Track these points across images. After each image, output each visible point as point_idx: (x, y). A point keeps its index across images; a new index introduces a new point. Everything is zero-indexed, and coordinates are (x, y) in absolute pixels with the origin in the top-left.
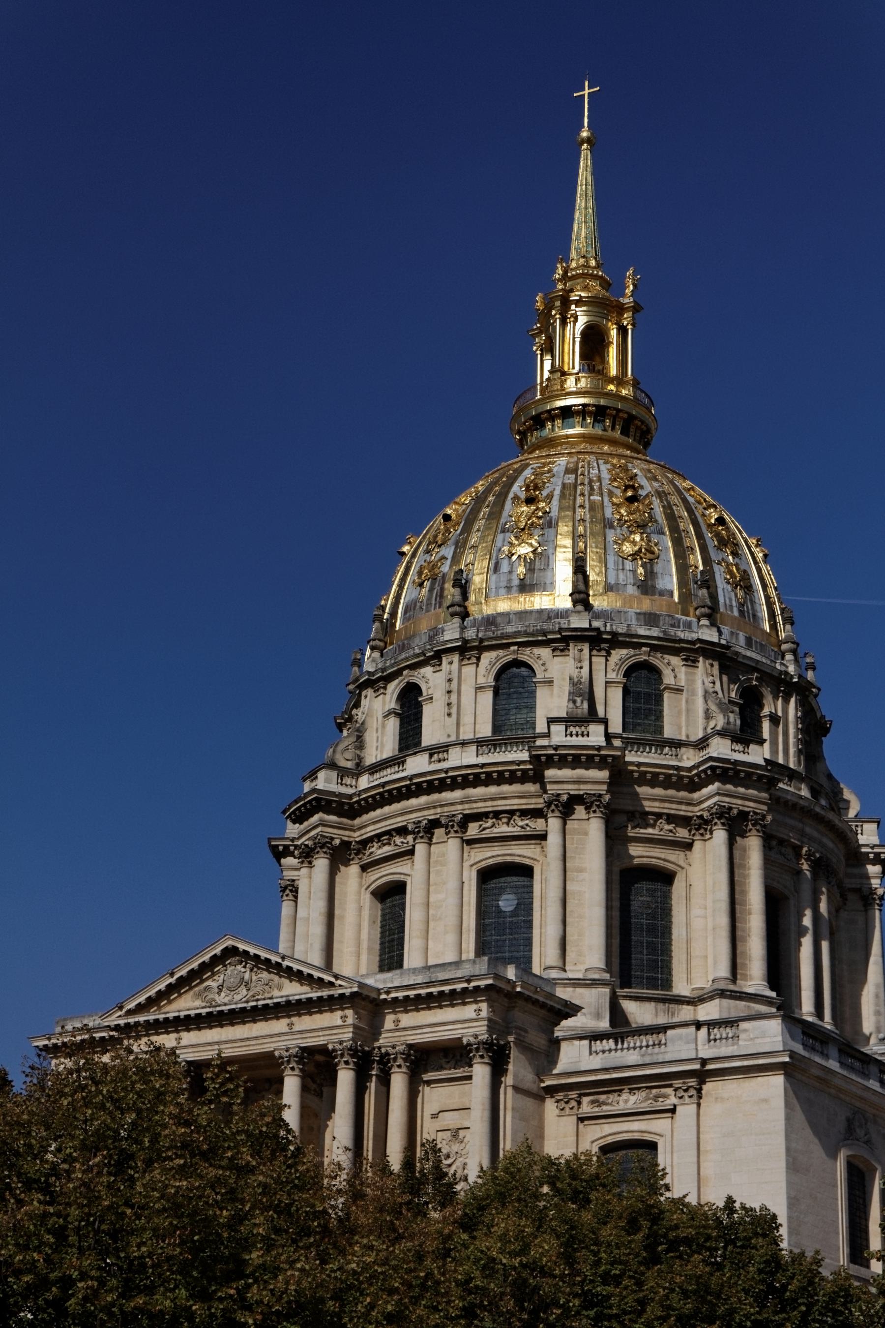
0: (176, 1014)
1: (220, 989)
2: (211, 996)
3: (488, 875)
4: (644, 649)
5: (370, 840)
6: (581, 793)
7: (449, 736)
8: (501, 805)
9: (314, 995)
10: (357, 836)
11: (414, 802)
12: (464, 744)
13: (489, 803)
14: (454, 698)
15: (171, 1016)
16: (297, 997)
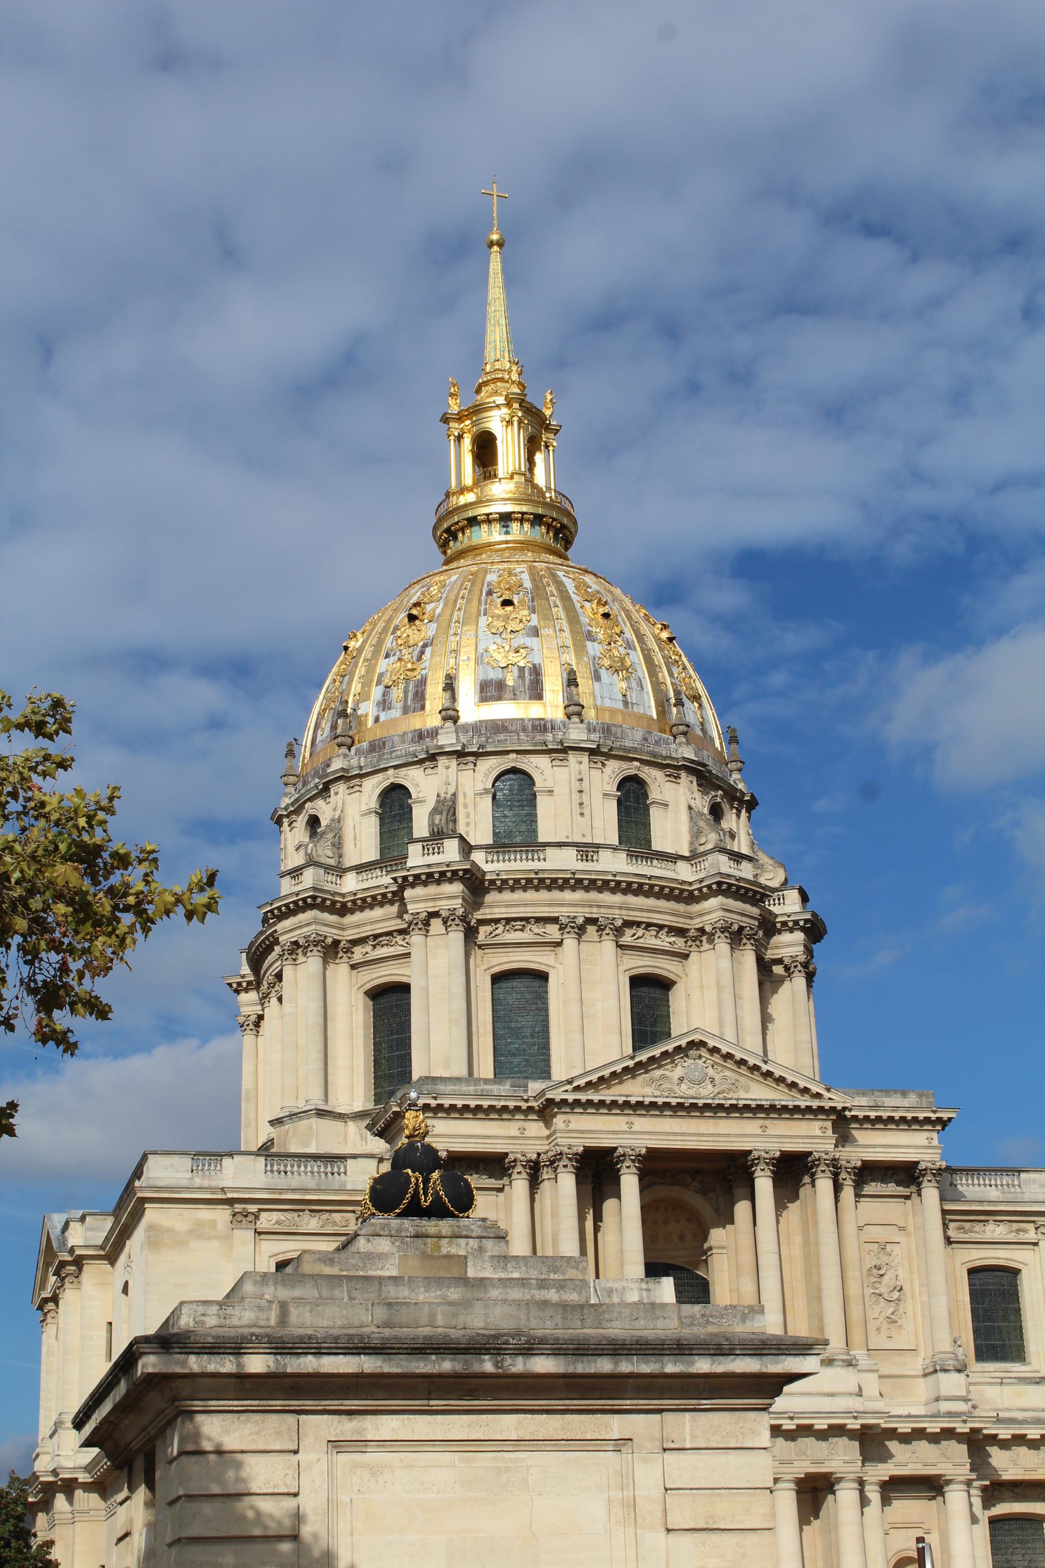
0: (641, 1099)
2: (666, 1086)
3: (639, 982)
4: (720, 792)
5: (497, 921)
6: (744, 925)
7: (584, 835)
9: (803, 1104)
10: (479, 915)
11: (567, 895)
13: (645, 914)
14: (585, 798)
15: (633, 1100)
16: (784, 1103)
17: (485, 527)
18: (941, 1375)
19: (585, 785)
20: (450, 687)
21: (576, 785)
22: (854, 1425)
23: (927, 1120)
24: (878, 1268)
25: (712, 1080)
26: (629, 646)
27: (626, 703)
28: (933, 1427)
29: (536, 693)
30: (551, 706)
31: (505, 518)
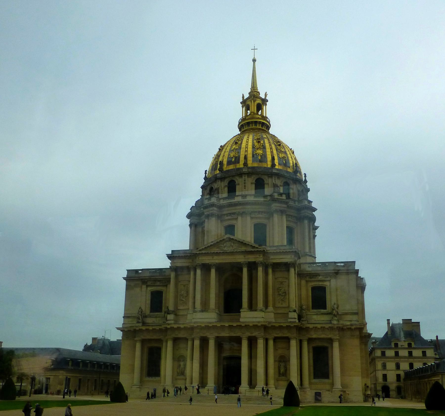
1: (225, 247)
3: (257, 226)
5: (224, 215)
8: (261, 210)
11: (238, 207)
12: (250, 195)
14: (246, 185)
15: (212, 252)
17: (245, 126)
18: (290, 313)
19: (246, 181)
20: (221, 163)
21: (243, 182)
22: (259, 324)
23: (289, 252)
24: (280, 288)
25: (232, 246)
26: (264, 148)
27: (260, 161)
28: (284, 325)
29: (239, 162)
30: (241, 165)
31: (248, 124)
